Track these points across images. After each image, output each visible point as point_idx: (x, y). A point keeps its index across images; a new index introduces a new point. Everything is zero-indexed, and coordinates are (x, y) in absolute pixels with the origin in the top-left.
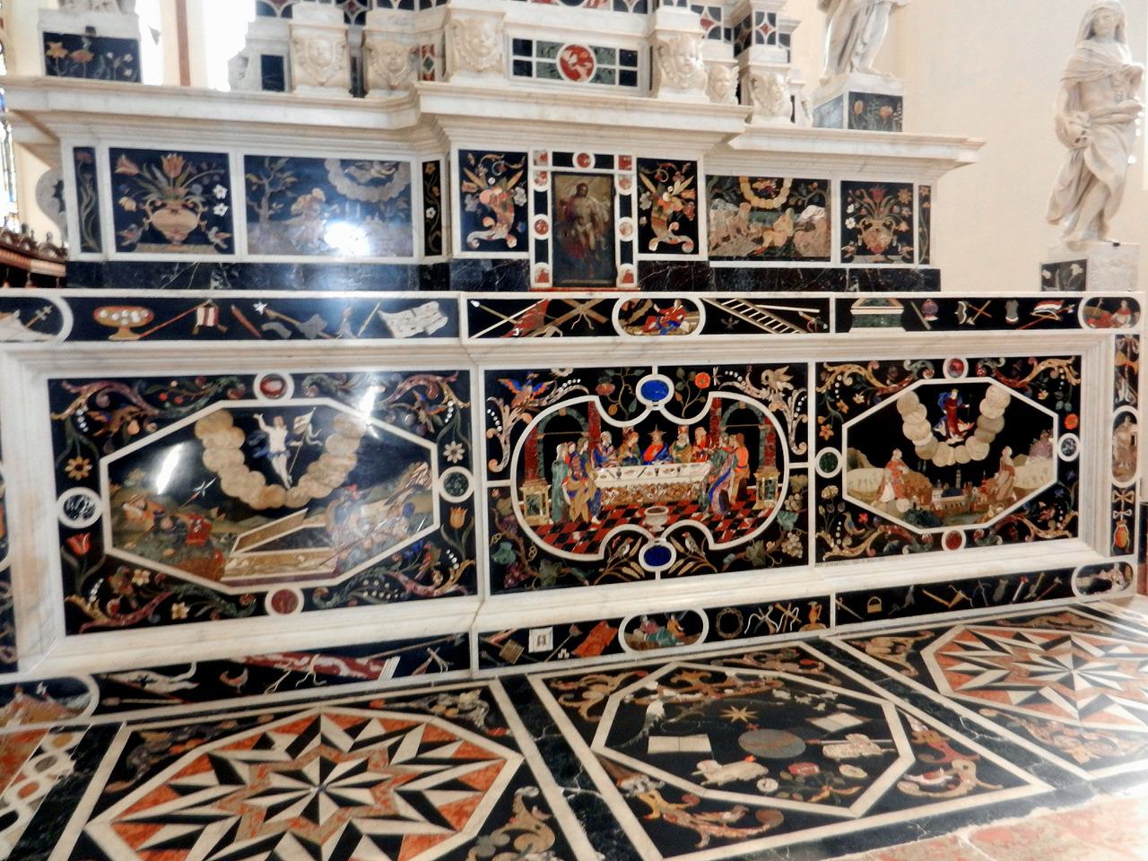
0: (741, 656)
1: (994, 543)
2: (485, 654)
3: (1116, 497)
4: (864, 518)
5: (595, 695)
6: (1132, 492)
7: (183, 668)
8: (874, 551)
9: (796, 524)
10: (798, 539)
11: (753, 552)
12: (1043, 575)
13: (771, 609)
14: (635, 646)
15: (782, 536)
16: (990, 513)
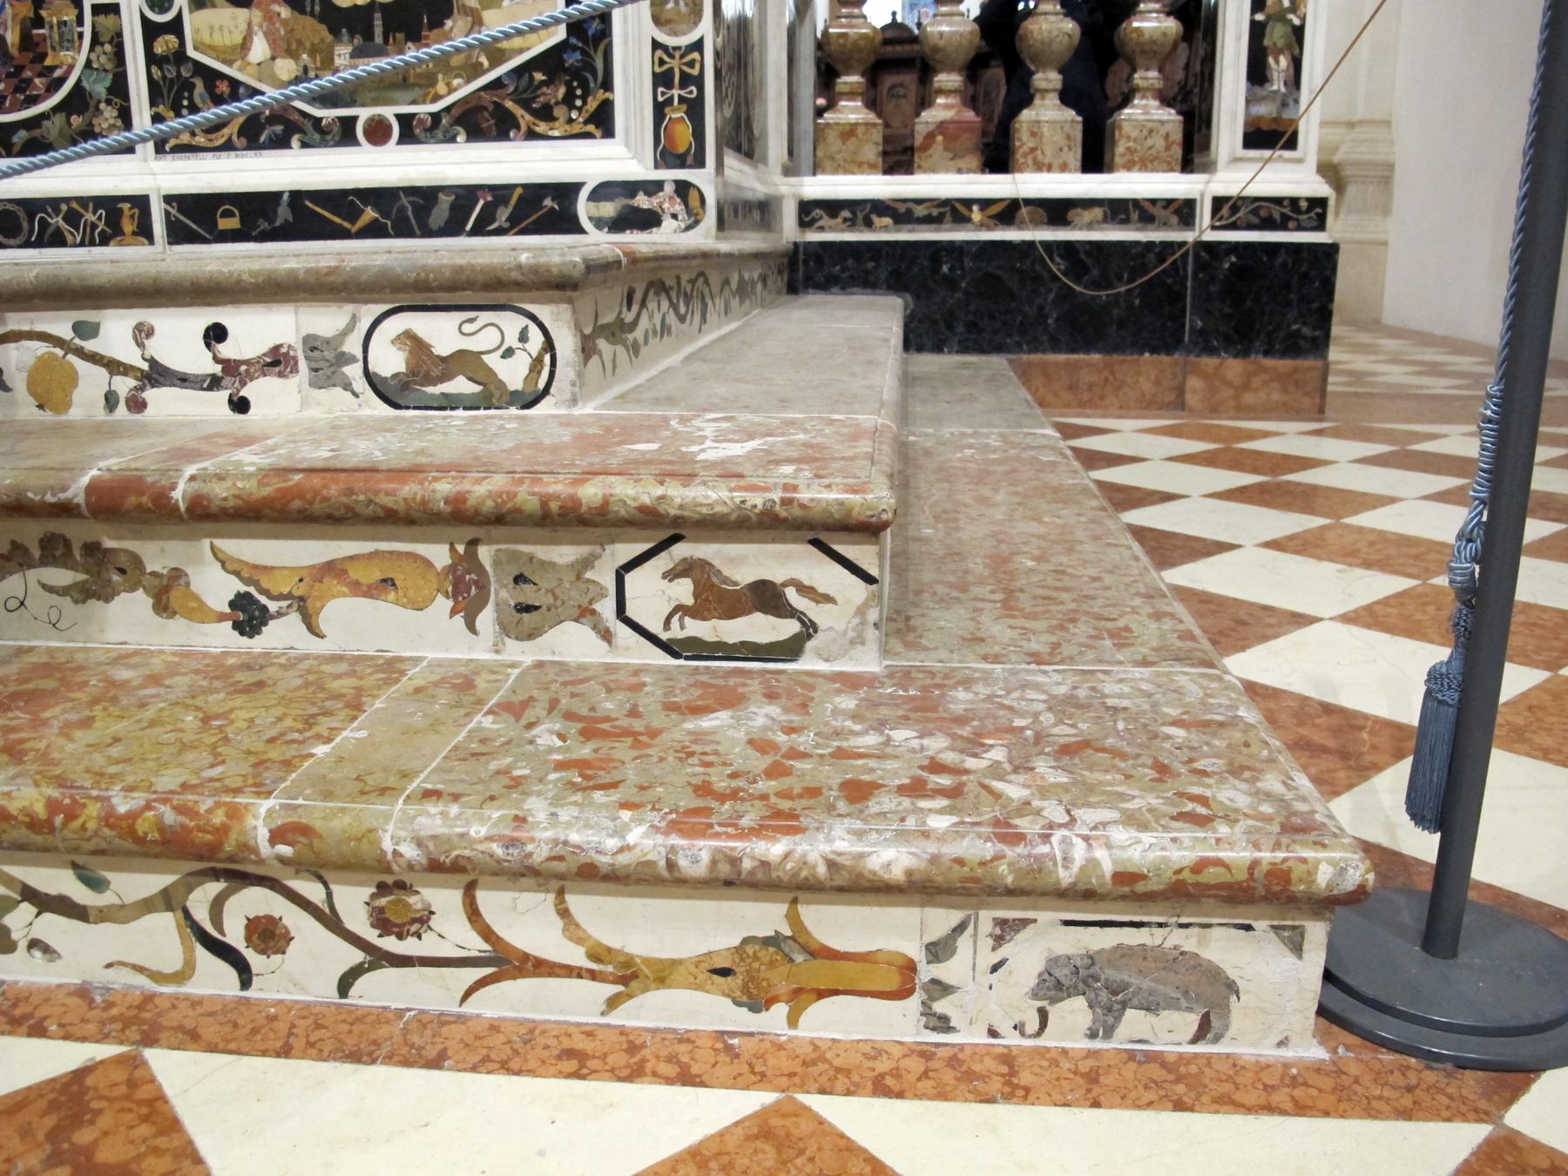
1: (452, 140)
3: (662, 62)
4: (223, 88)
6: (696, 55)
8: (244, 142)
9: (110, 90)
10: (115, 113)
11: (53, 128)
12: (519, 191)
13: (64, 207)
15: (92, 109)
16: (441, 88)
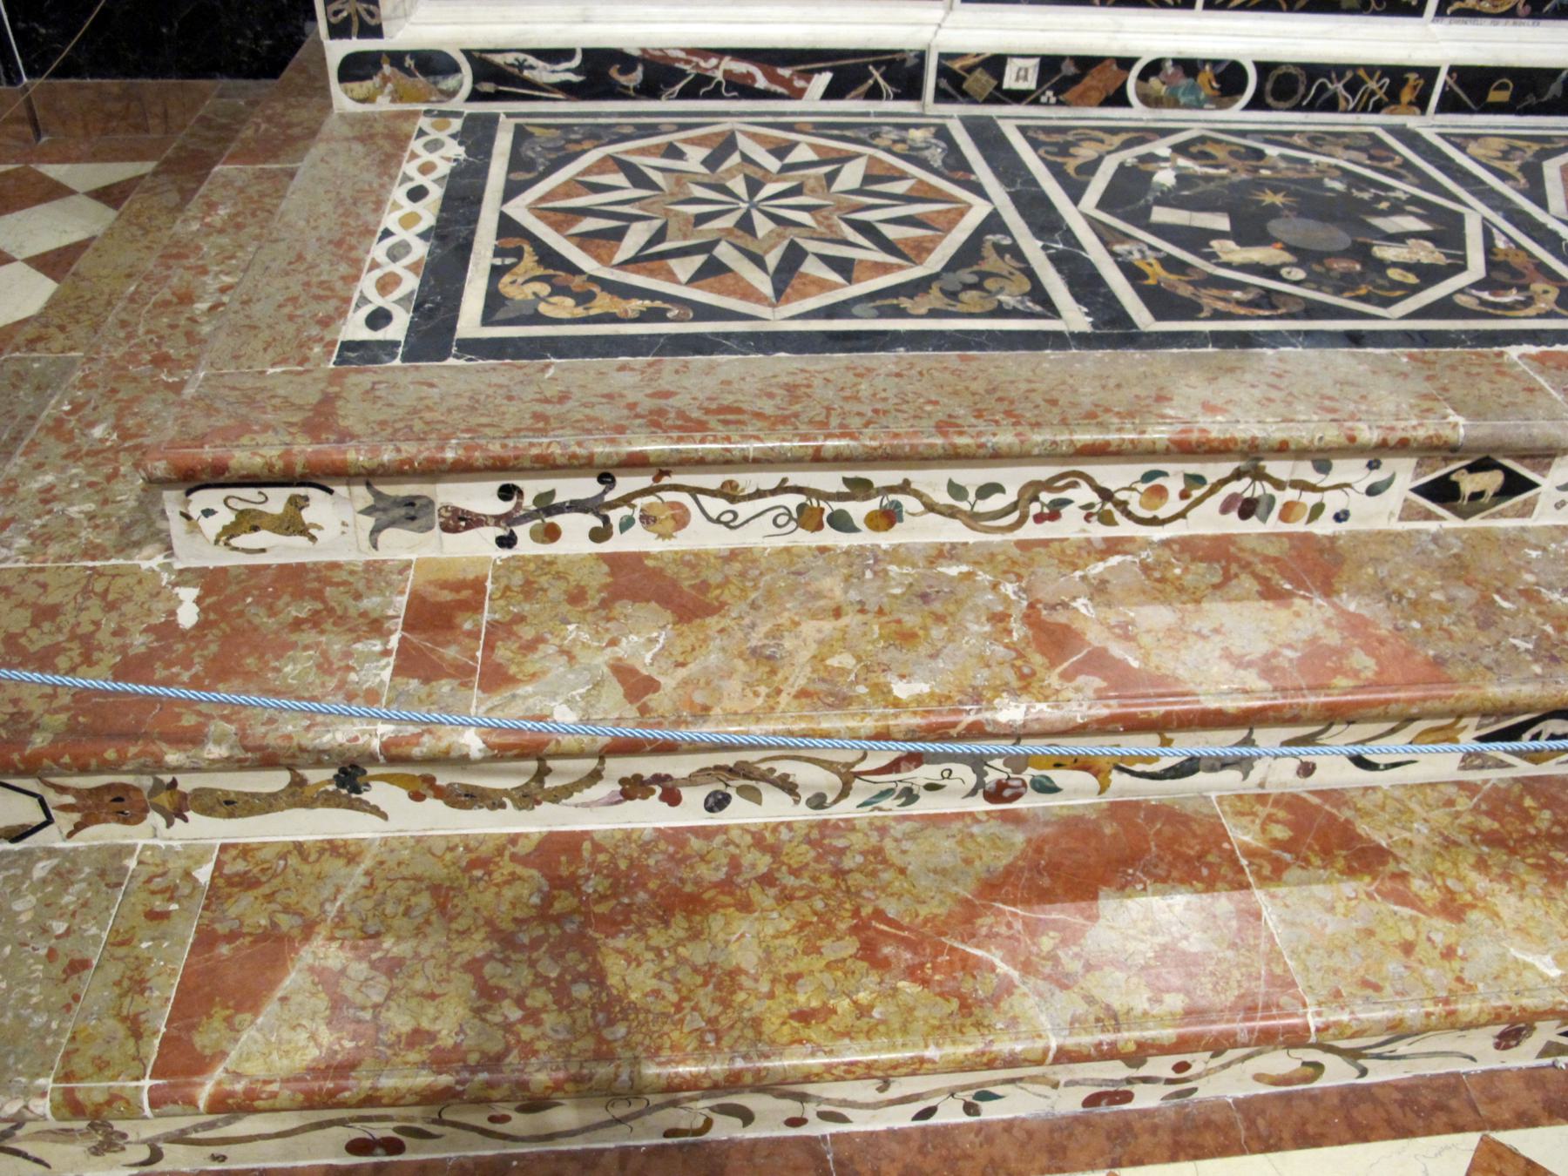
0: (1290, 134)
2: (944, 83)
5: (1087, 152)
7: (567, 54)
14: (1149, 101)
